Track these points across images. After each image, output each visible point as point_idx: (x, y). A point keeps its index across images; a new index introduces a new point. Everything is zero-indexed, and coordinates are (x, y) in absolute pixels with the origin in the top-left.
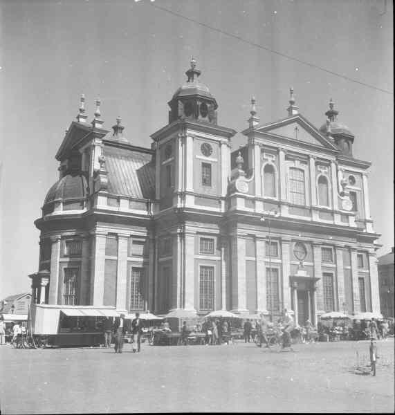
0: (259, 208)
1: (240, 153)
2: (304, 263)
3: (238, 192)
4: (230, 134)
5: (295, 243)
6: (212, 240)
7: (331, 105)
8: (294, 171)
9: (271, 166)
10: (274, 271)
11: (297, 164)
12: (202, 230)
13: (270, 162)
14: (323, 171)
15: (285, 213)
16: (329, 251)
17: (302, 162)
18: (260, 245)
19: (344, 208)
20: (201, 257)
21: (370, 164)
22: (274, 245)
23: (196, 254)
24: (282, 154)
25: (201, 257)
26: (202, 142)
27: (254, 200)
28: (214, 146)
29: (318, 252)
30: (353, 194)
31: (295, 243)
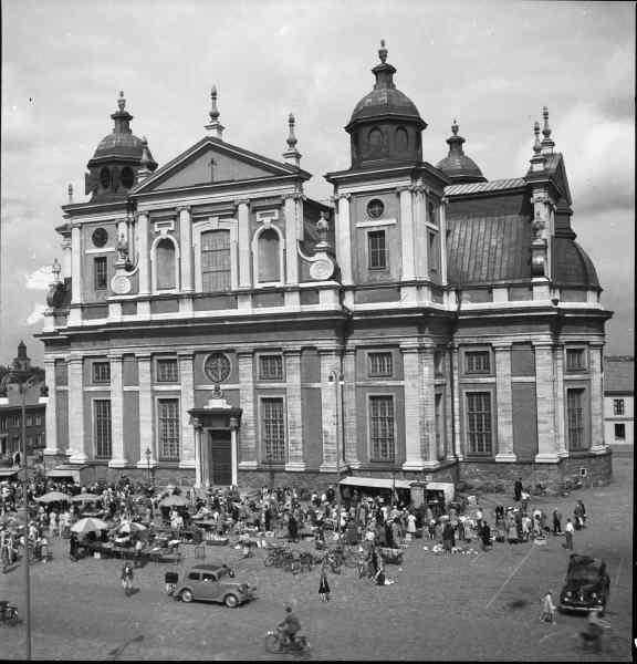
0: (144, 313)
2: (222, 387)
5: (206, 357)
7: (383, 55)
8: (211, 237)
9: (168, 241)
10: (169, 403)
11: (214, 223)
13: (164, 234)
14: (267, 220)
15: (186, 312)
16: (271, 363)
17: (220, 217)
18: (144, 367)
19: (314, 277)
20: (93, 389)
22: (166, 366)
23: (85, 384)
24: (185, 216)
25: (93, 389)
27: (135, 302)
28: (109, 228)
29: (246, 368)
30: (377, 237)
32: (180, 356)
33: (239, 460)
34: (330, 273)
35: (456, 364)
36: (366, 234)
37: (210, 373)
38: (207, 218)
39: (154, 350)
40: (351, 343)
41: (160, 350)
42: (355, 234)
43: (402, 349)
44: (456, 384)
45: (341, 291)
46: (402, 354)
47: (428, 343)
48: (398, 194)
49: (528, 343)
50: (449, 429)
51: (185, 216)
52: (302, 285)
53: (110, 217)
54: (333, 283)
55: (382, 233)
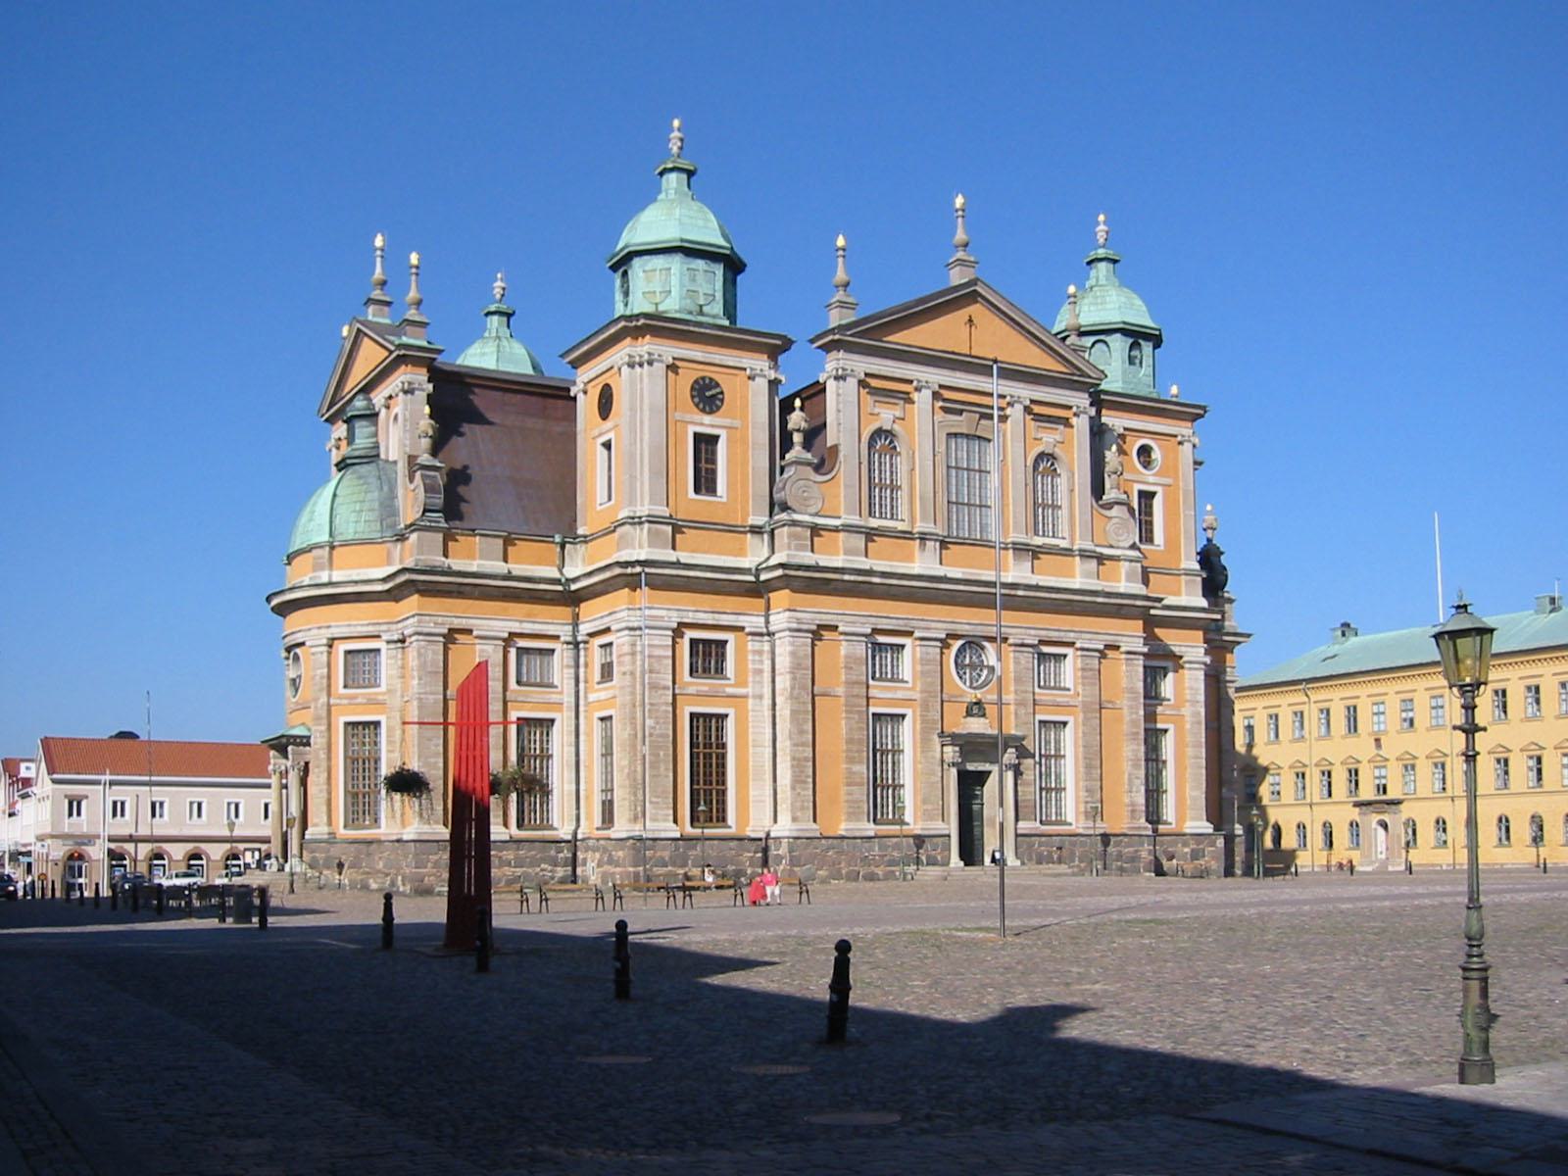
1: (798, 403)
3: (794, 511)
4: (776, 348)
5: (960, 642)
6: (723, 643)
12: (689, 618)
21: (1204, 408)
24: (923, 399)
26: (687, 377)
31: (960, 642)
33: (1017, 820)
38: (960, 412)
51: (923, 399)
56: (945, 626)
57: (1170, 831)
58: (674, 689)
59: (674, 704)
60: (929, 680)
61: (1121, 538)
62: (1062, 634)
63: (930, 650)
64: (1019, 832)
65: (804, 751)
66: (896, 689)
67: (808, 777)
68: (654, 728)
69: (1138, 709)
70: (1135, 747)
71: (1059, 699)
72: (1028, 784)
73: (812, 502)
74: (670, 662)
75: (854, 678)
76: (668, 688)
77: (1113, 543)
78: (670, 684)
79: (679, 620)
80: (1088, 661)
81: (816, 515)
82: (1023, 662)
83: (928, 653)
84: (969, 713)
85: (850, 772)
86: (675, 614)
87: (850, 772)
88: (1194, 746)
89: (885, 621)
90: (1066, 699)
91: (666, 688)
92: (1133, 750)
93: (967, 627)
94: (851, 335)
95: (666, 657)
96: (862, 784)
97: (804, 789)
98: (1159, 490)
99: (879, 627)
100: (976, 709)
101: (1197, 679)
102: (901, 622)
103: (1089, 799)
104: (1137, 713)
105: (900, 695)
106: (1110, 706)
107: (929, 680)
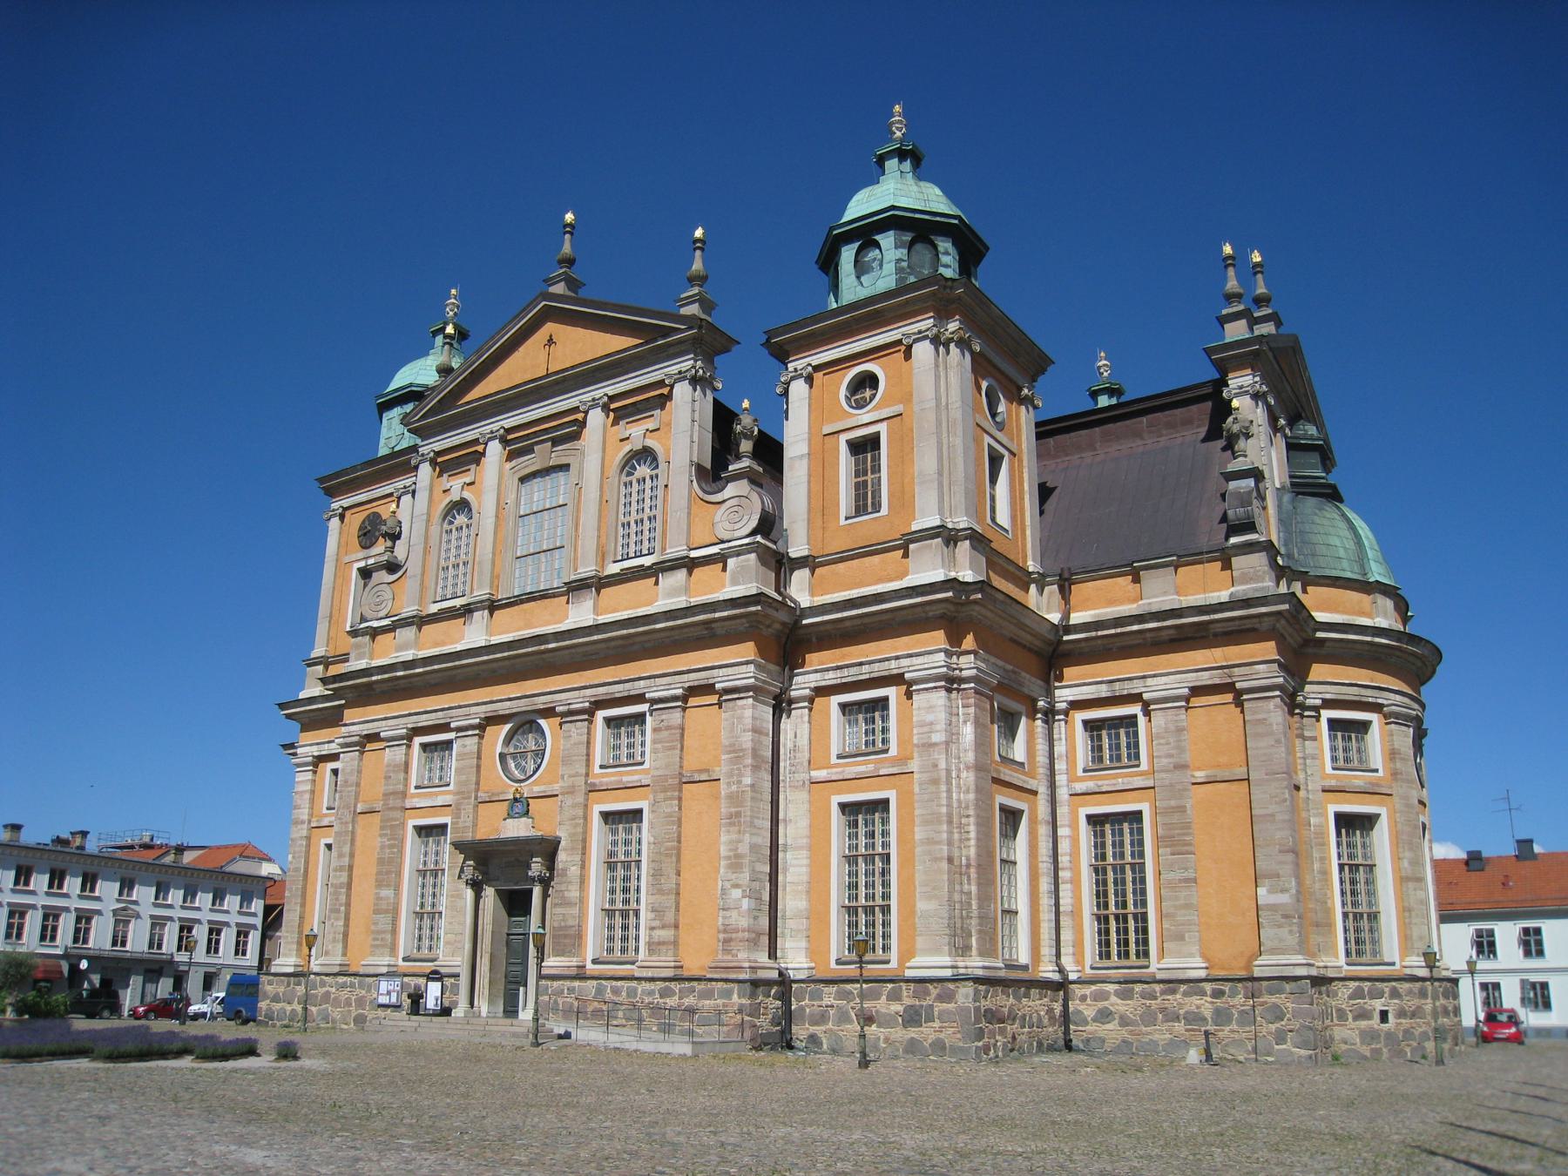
5: (508, 727)
17: (556, 442)
26: (356, 520)
28: (385, 510)
31: (508, 727)
32: (459, 729)
34: (754, 523)
35: (1060, 748)
36: (843, 448)
37: (512, 765)
39: (412, 722)
40: (803, 683)
41: (424, 720)
42: (822, 442)
43: (910, 684)
44: (1063, 793)
45: (781, 565)
46: (909, 695)
47: (968, 665)
48: (909, 347)
49: (1228, 687)
50: (1046, 902)
52: (694, 554)
53: (388, 490)
54: (759, 538)
55: (871, 443)
56: (483, 708)
57: (889, 975)
58: (310, 822)
59: (308, 838)
60: (464, 777)
61: (736, 527)
62: (628, 686)
63: (468, 741)
64: (545, 971)
65: (341, 876)
66: (436, 794)
67: (341, 905)
68: (291, 863)
69: (741, 775)
70: (734, 837)
71: (625, 779)
72: (569, 904)
73: (383, 606)
74: (307, 796)
75: (391, 788)
76: (303, 822)
77: (726, 536)
78: (306, 817)
79: (316, 754)
80: (665, 716)
81: (387, 617)
82: (574, 735)
83: (465, 746)
84: (510, 816)
85: (379, 898)
86: (315, 748)
87: (379, 898)
88: (926, 822)
89: (424, 717)
90: (636, 778)
91: (303, 822)
92: (731, 842)
93: (508, 703)
94: (418, 420)
95: (305, 792)
96: (386, 911)
97: (337, 919)
98: (882, 428)
99: (420, 725)
100: (520, 806)
101: (931, 708)
102: (440, 714)
103: (657, 923)
104: (740, 782)
105: (440, 801)
106: (704, 777)
107: (464, 777)
